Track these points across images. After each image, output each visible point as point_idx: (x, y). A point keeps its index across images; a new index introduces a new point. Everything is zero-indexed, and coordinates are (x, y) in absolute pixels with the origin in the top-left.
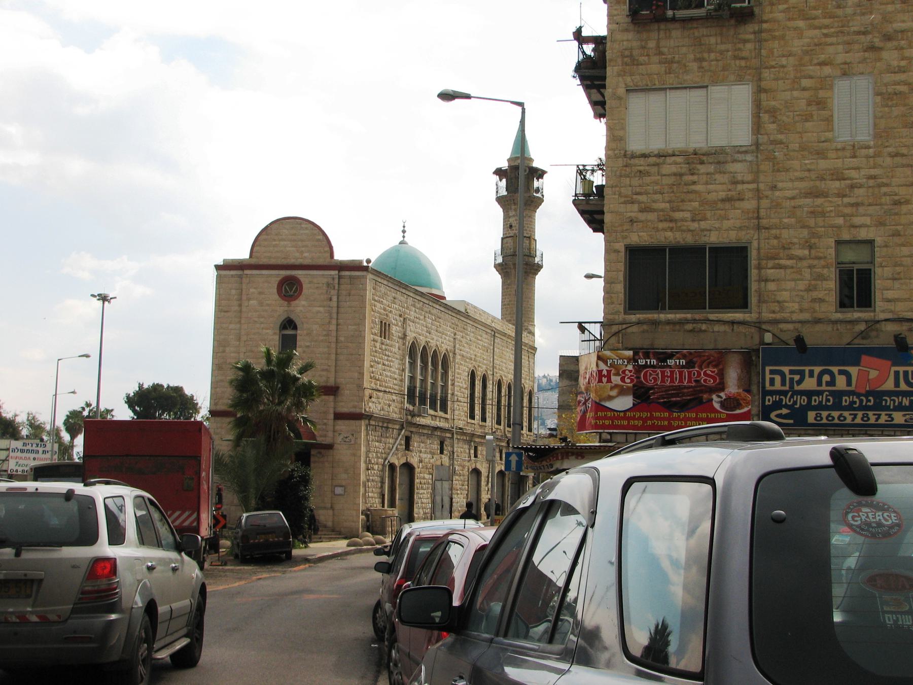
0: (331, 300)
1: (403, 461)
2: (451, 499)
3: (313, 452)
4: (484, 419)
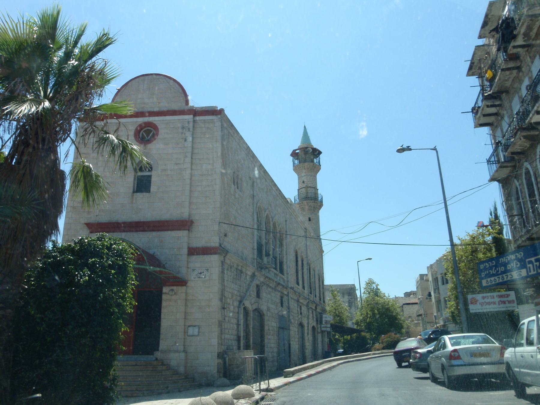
0: (186, 140)
1: (255, 307)
2: (290, 345)
3: (165, 290)
4: (304, 287)
